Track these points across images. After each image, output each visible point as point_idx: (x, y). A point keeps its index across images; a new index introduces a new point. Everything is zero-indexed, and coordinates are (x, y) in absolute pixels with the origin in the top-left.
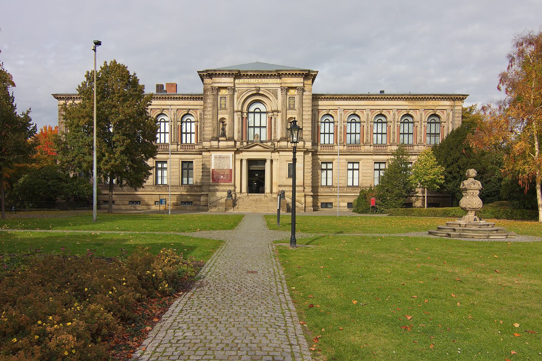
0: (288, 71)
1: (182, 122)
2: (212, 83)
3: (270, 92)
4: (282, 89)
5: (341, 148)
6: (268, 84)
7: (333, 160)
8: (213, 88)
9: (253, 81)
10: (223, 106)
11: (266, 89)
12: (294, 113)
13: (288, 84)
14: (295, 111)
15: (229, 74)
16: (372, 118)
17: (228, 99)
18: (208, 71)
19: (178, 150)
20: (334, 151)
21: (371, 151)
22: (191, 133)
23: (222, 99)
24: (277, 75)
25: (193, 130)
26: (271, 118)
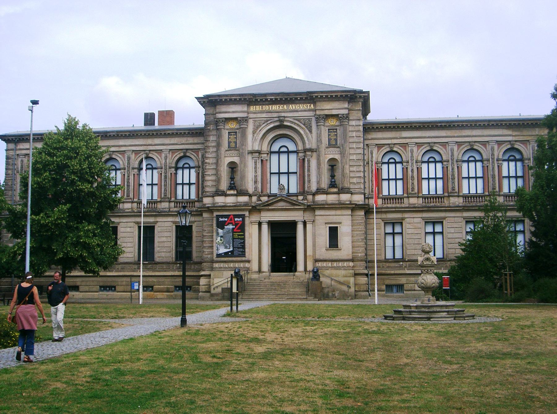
0: (324, 93)
1: (177, 169)
2: (217, 113)
3: (301, 123)
5: (413, 201)
7: (403, 219)
9: (275, 107)
10: (233, 145)
12: (337, 153)
13: (326, 111)
14: (338, 149)
15: (240, 99)
16: (458, 155)
17: (239, 135)
18: (210, 97)
19: (171, 210)
20: (403, 205)
21: (461, 205)
22: (190, 184)
25: (193, 180)
26: (304, 160)
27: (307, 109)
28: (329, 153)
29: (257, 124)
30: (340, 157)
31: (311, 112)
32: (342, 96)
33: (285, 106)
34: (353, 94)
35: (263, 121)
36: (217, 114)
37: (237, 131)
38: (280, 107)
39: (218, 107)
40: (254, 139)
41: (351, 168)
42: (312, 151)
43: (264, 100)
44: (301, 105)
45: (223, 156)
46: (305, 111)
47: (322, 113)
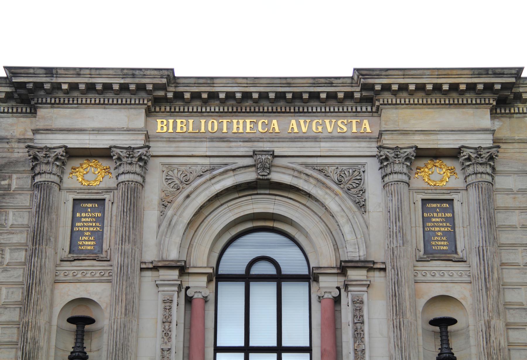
0: (413, 76)
2: (36, 131)
3: (327, 176)
4: (387, 159)
6: (315, 139)
8: (41, 155)
11: (306, 165)
12: (456, 278)
13: (417, 137)
15: (124, 88)
23: (85, 210)
24: (357, 95)
26: (337, 300)
27: (349, 134)
28: (429, 277)
29: (176, 175)
30: (467, 294)
31: (363, 144)
32: (471, 87)
33: (275, 122)
34: (513, 80)
35: (199, 167)
36: (38, 136)
37: (107, 196)
38: (256, 123)
39: (42, 112)
40: (165, 224)
41: (511, 333)
42: (370, 269)
43: (205, 96)
44: (327, 121)
45: (48, 278)
46: (343, 138)
47: (403, 142)
